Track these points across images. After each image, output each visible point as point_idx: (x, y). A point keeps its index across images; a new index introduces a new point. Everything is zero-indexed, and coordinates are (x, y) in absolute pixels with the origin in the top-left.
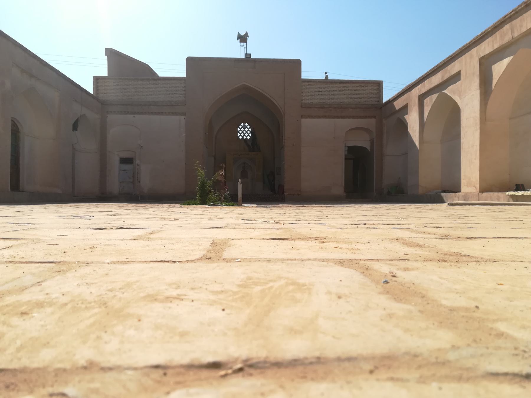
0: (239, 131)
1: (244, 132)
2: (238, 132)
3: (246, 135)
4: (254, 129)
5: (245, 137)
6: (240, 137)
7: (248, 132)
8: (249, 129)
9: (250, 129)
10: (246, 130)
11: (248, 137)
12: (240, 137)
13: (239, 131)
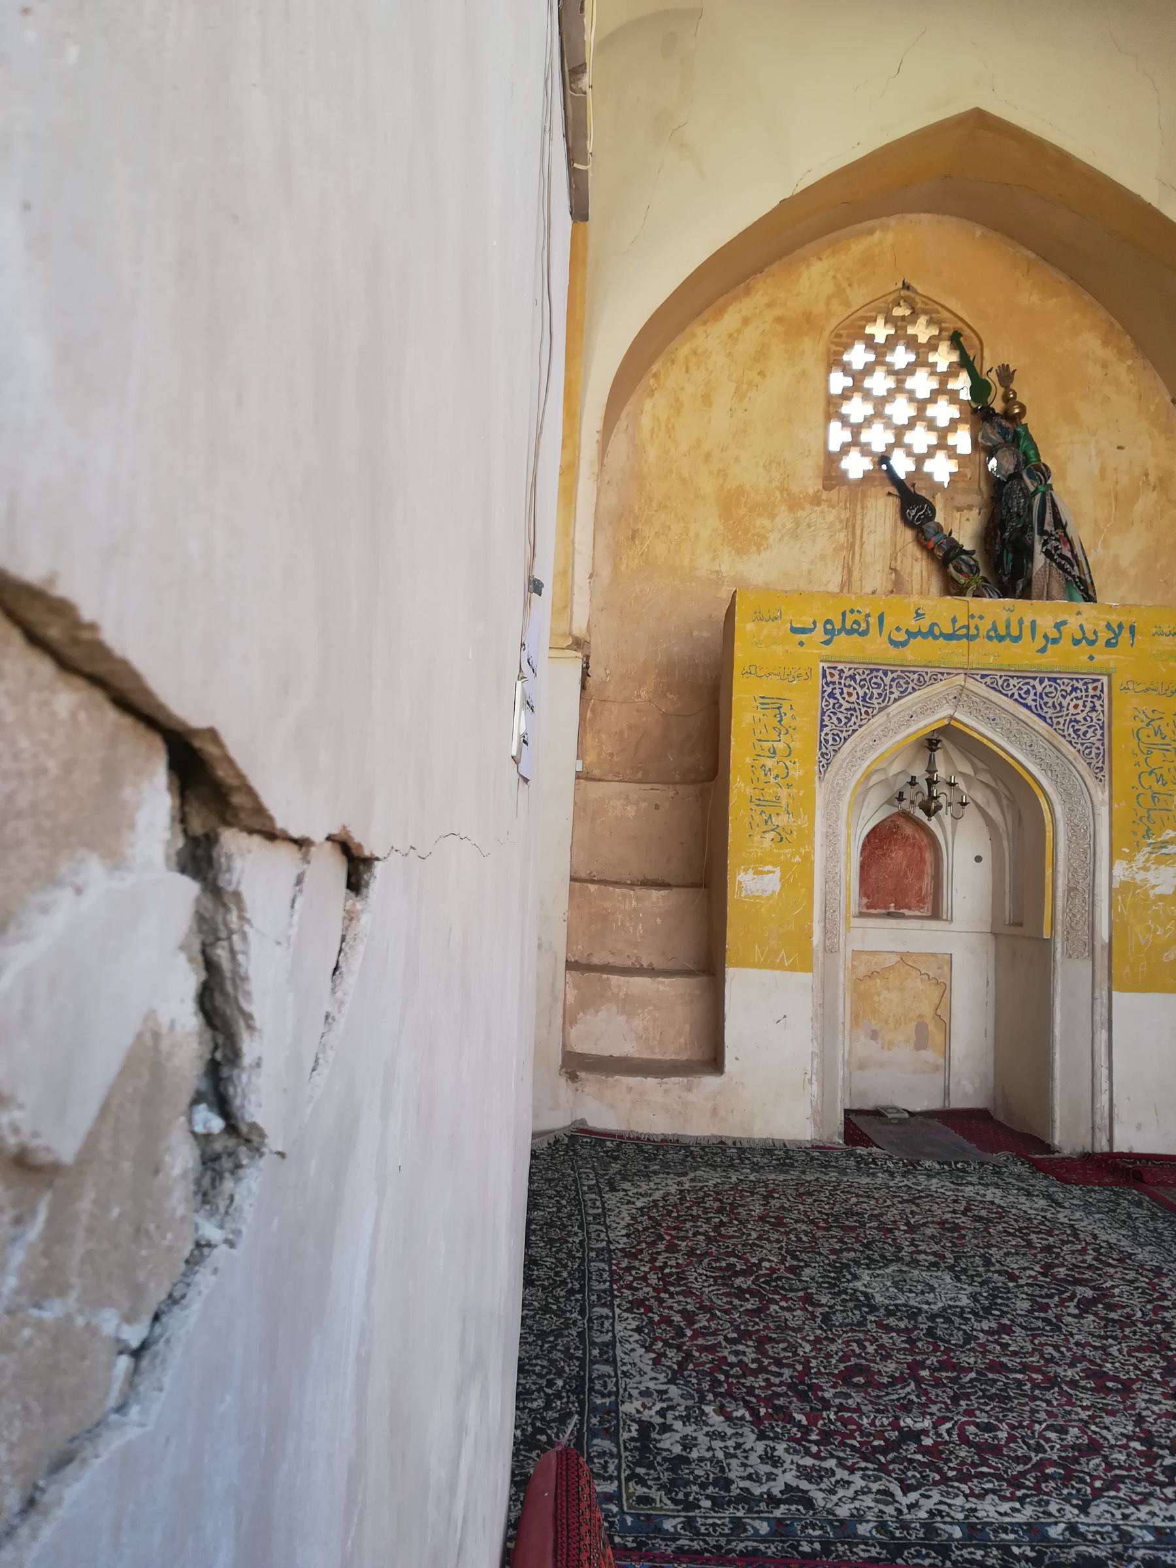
0: (846, 395)
1: (900, 410)
2: (832, 408)
3: (920, 439)
4: (1006, 375)
5: (911, 466)
6: (856, 466)
7: (943, 412)
8: (952, 385)
9: (962, 384)
10: (923, 393)
11: (941, 469)
12: (856, 466)
13: (846, 395)
